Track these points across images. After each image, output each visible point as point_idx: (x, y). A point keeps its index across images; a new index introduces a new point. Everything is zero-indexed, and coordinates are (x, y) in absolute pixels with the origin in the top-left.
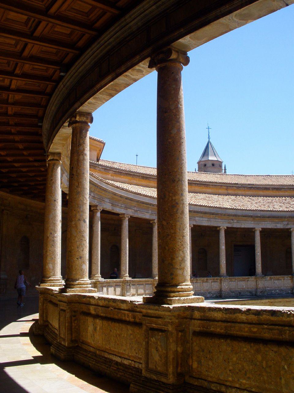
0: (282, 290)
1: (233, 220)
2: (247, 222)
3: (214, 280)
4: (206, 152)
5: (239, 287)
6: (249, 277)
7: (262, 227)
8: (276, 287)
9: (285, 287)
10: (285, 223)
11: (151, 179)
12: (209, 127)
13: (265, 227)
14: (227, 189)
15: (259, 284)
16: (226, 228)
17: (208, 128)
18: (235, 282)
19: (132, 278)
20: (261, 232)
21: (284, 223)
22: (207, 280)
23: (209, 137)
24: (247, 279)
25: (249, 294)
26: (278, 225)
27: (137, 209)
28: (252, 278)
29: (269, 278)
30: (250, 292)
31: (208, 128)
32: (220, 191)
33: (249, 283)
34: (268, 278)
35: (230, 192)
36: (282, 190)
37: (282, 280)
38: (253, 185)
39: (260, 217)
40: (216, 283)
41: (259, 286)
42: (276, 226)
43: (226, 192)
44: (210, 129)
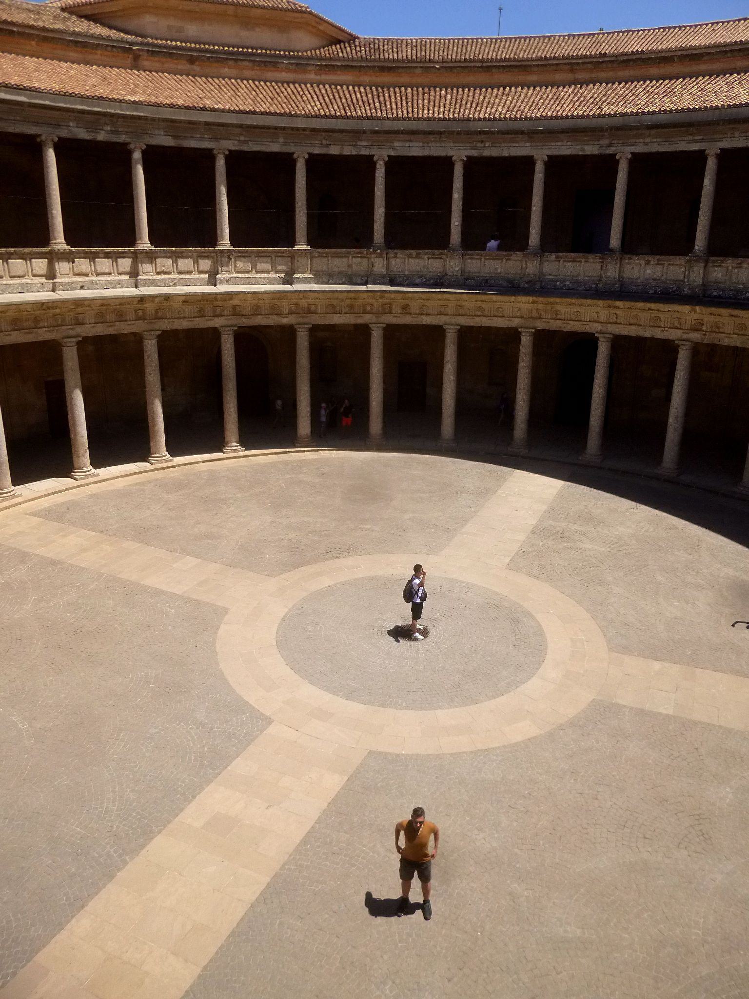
1: (482, 142)
2: (514, 145)
3: (434, 254)
7: (550, 153)
10: (605, 142)
11: (400, 70)
13: (556, 153)
14: (572, 71)
16: (465, 159)
18: (478, 261)
21: (601, 142)
22: (418, 254)
24: (505, 256)
25: (505, 284)
26: (586, 147)
27: (247, 139)
28: (519, 255)
30: (510, 281)
32: (558, 77)
35: (580, 76)
36: (705, 58)
39: (542, 132)
40: (438, 260)
42: (583, 150)
43: (570, 76)
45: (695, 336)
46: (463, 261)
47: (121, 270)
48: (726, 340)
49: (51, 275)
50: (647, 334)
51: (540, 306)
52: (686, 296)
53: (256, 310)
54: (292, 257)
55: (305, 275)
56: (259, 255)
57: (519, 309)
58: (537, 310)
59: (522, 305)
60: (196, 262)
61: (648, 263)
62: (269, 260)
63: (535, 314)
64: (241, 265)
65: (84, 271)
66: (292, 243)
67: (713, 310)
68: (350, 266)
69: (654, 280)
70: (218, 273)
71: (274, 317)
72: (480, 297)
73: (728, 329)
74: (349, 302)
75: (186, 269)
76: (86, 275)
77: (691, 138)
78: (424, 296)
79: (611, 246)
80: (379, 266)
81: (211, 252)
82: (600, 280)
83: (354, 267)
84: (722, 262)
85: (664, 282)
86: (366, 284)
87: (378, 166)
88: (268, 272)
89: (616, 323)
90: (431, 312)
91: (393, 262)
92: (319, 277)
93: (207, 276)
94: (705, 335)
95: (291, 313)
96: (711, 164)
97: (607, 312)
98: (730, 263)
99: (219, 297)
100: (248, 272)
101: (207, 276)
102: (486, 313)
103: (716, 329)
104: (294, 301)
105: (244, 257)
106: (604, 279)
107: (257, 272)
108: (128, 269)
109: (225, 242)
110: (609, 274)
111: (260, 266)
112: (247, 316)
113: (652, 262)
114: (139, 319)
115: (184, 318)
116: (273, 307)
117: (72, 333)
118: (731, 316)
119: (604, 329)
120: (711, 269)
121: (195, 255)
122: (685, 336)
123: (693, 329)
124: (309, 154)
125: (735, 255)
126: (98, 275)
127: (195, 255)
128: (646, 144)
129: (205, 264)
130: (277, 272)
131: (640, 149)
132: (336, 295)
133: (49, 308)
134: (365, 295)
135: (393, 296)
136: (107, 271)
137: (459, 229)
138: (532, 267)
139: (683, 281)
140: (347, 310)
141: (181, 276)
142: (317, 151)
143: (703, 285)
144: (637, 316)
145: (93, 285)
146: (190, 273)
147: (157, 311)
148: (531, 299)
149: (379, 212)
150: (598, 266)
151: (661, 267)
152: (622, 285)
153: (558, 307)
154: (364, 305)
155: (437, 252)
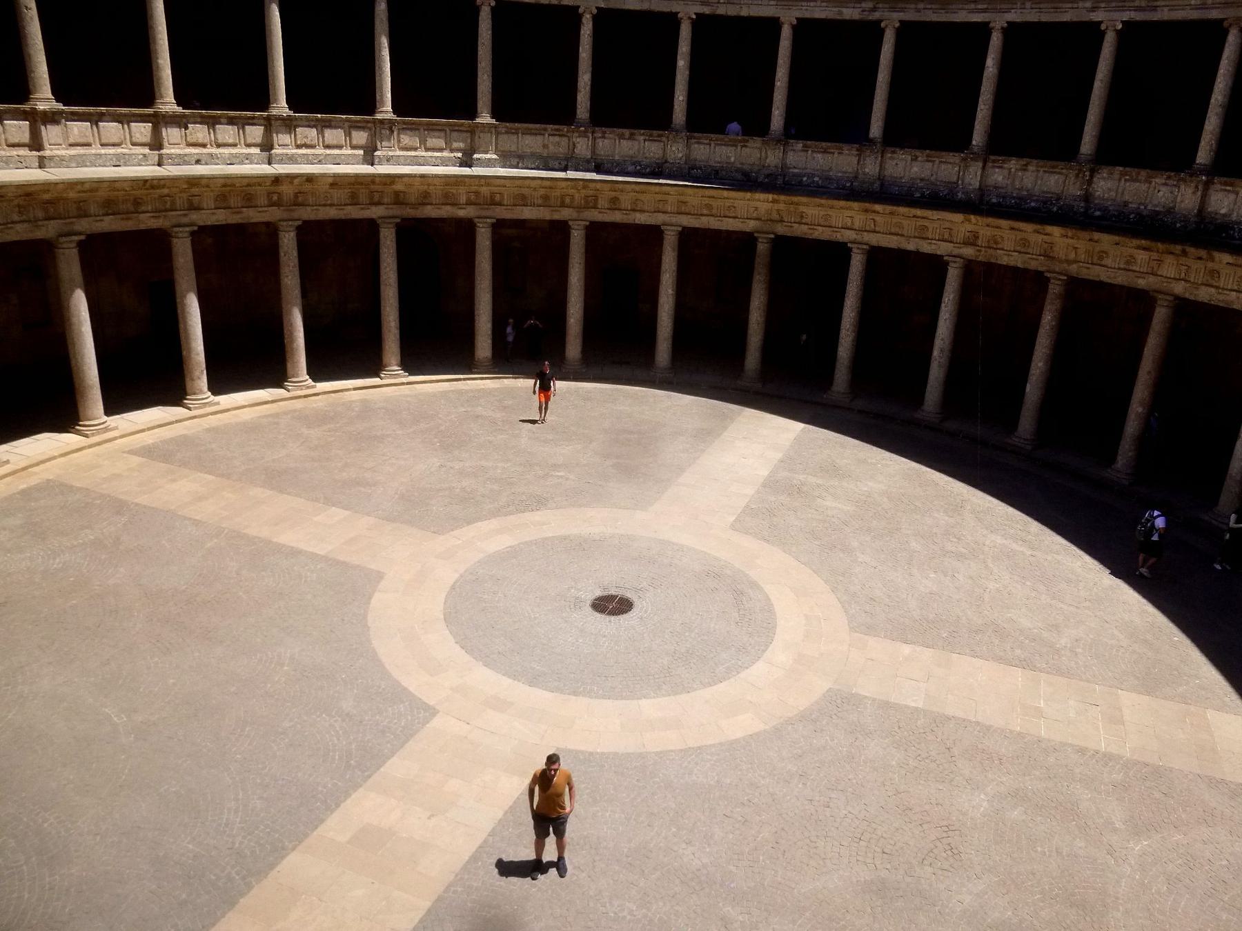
0: (828, 179)
5: (718, 159)
13: (807, 15)
21: (863, 5)
22: (632, 134)
25: (739, 176)
26: (844, 10)
30: (746, 174)
40: (656, 144)
42: (840, 13)
45: (968, 252)
46: (688, 146)
47: (249, 141)
48: (1006, 258)
49: (156, 144)
50: (911, 247)
51: (781, 206)
52: (960, 201)
53: (425, 199)
54: (472, 131)
55: (488, 156)
56: (430, 128)
57: (756, 209)
58: (778, 211)
59: (758, 204)
60: (348, 134)
61: (915, 159)
62: (442, 134)
63: (775, 216)
64: (406, 139)
65: (200, 141)
66: (472, 113)
67: (990, 220)
68: (545, 146)
69: (922, 180)
70: (376, 149)
71: (448, 208)
72: (707, 192)
73: (1008, 245)
74: (542, 192)
75: (335, 142)
76: (204, 146)
77: (973, 6)
78: (637, 188)
79: (871, 135)
80: (583, 147)
81: (368, 122)
82: (856, 177)
83: (551, 147)
84: (1004, 161)
85: (933, 184)
86: (565, 169)
87: (584, 20)
88: (441, 150)
89: (875, 232)
90: (646, 208)
91: (600, 143)
92: (507, 158)
93: (362, 152)
95: (469, 203)
96: (996, 40)
97: (863, 217)
98: (1013, 164)
99: (377, 180)
100: (416, 149)
101: (362, 152)
102: (714, 211)
103: (994, 244)
104: (474, 188)
105: (411, 129)
107: (427, 150)
108: (259, 140)
109: (386, 109)
111: (431, 142)
112: (414, 206)
114: (272, 204)
115: (331, 205)
116: (446, 196)
117: (185, 220)
118: (1012, 229)
119: (859, 238)
120: (990, 171)
121: (347, 124)
122: (956, 251)
123: (967, 243)
125: (1019, 155)
126: (219, 146)
127: (347, 124)
128: (918, 11)
129: (360, 137)
130: (452, 151)
131: (910, 16)
132: (527, 182)
133: (153, 187)
134: (564, 184)
135: (599, 186)
136: (231, 141)
137: (684, 105)
138: (773, 157)
139: (957, 183)
140: (540, 202)
141: (328, 152)
143: (980, 189)
144: (900, 226)
145: (212, 159)
146: (340, 147)
147: (296, 195)
148: (770, 197)
149: (585, 79)
150: (855, 160)
152: (882, 185)
153: (802, 208)
154: (563, 197)
155: (655, 133)
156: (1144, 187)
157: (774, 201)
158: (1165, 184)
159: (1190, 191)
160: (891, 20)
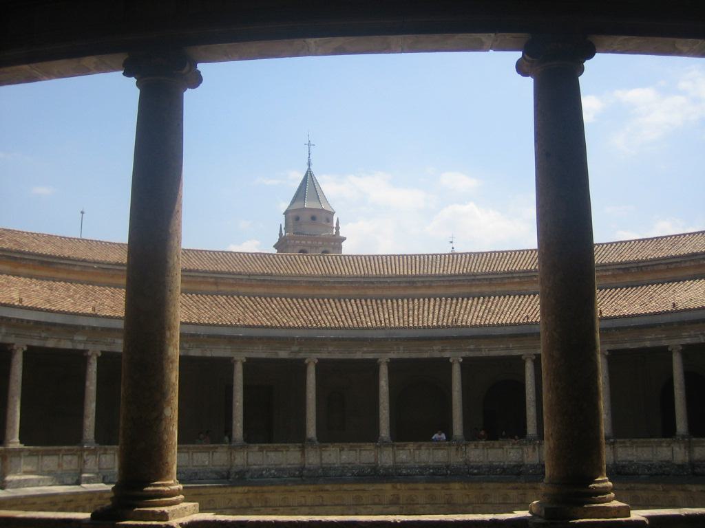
4: (301, 194)
5: (195, 464)
6: (216, 445)
8: (272, 465)
9: (289, 464)
10: (295, 348)
12: (307, 146)
13: (254, 355)
15: (235, 459)
17: (309, 145)
18: (186, 455)
19: (25, 446)
20: (244, 365)
23: (309, 162)
29: (257, 448)
30: (217, 473)
31: (309, 145)
33: (217, 456)
34: (256, 447)
37: (285, 452)
38: (271, 275)
41: (236, 461)
44: (312, 147)
57: (231, 500)
58: (247, 499)
68: (60, 465)
69: (349, 464)
77: (365, 349)
78: (196, 491)
84: (405, 446)
87: (91, 361)
89: (322, 505)
94: (401, 507)
96: (384, 371)
98: (411, 446)
106: (307, 466)
109: (15, 442)
110: (310, 461)
113: (346, 449)
118: (426, 489)
124: (28, 346)
128: (329, 352)
142: (36, 343)
150: (298, 454)
151: (354, 452)
156: (500, 451)
157: (249, 492)
158: (513, 448)
159: (530, 450)
160: (312, 359)
